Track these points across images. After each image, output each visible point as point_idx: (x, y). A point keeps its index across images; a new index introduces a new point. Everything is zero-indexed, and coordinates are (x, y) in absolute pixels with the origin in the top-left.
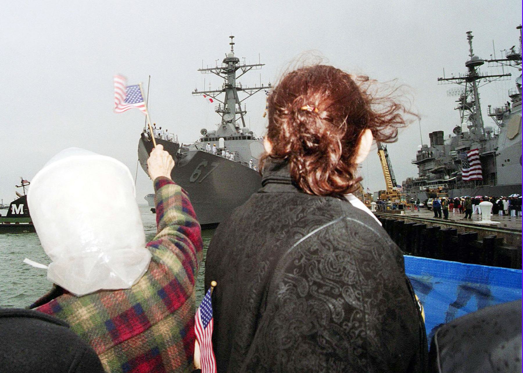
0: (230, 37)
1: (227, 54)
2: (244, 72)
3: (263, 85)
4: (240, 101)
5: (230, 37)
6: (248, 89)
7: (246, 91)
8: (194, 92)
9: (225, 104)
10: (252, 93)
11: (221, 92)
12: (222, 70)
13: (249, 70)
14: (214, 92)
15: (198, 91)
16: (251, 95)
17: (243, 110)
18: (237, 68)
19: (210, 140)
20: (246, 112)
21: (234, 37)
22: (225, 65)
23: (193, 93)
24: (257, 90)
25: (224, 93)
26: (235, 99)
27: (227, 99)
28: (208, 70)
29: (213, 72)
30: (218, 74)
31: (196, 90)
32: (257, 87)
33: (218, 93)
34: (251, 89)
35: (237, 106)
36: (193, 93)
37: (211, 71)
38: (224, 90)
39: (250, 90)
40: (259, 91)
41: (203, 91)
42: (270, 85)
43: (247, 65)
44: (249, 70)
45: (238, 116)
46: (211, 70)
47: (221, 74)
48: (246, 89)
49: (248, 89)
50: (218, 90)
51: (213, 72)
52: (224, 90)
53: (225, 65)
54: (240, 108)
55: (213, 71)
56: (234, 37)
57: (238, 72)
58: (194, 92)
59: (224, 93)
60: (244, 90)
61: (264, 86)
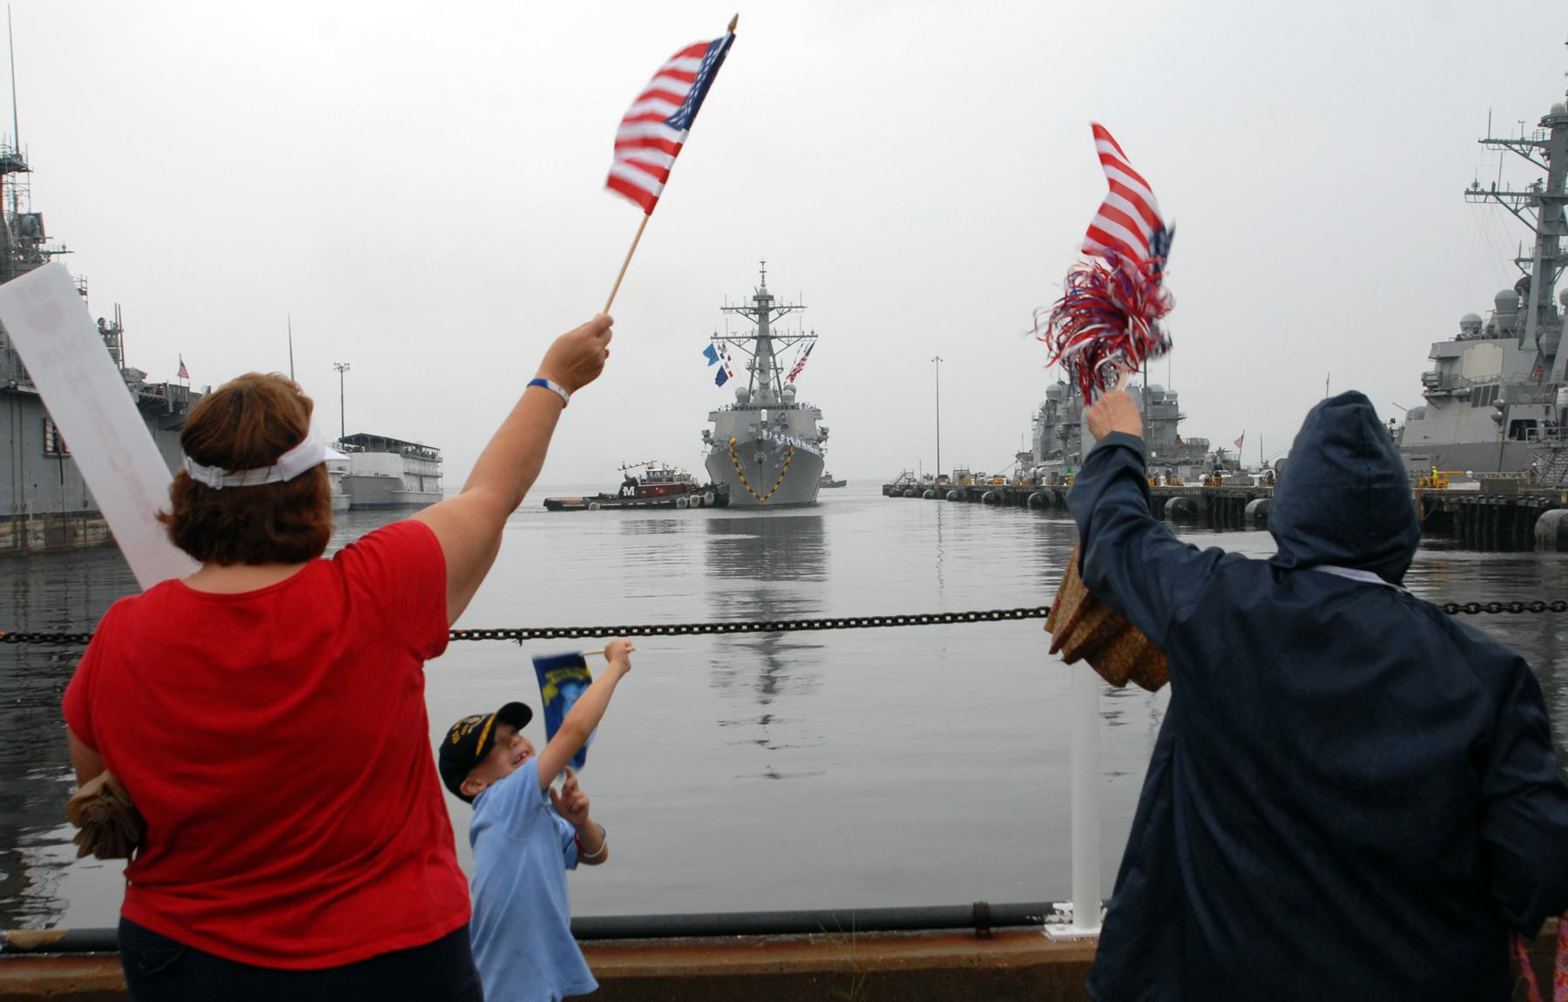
2: (781, 315)
4: (775, 352)
11: (750, 338)
15: (718, 336)
16: (789, 345)
17: (779, 366)
19: (747, 409)
22: (756, 305)
25: (756, 341)
30: (747, 315)
31: (716, 334)
33: (745, 340)
36: (712, 338)
41: (725, 336)
42: (812, 333)
43: (784, 305)
45: (772, 373)
46: (737, 309)
47: (750, 316)
53: (756, 305)
60: (779, 338)
61: (805, 334)
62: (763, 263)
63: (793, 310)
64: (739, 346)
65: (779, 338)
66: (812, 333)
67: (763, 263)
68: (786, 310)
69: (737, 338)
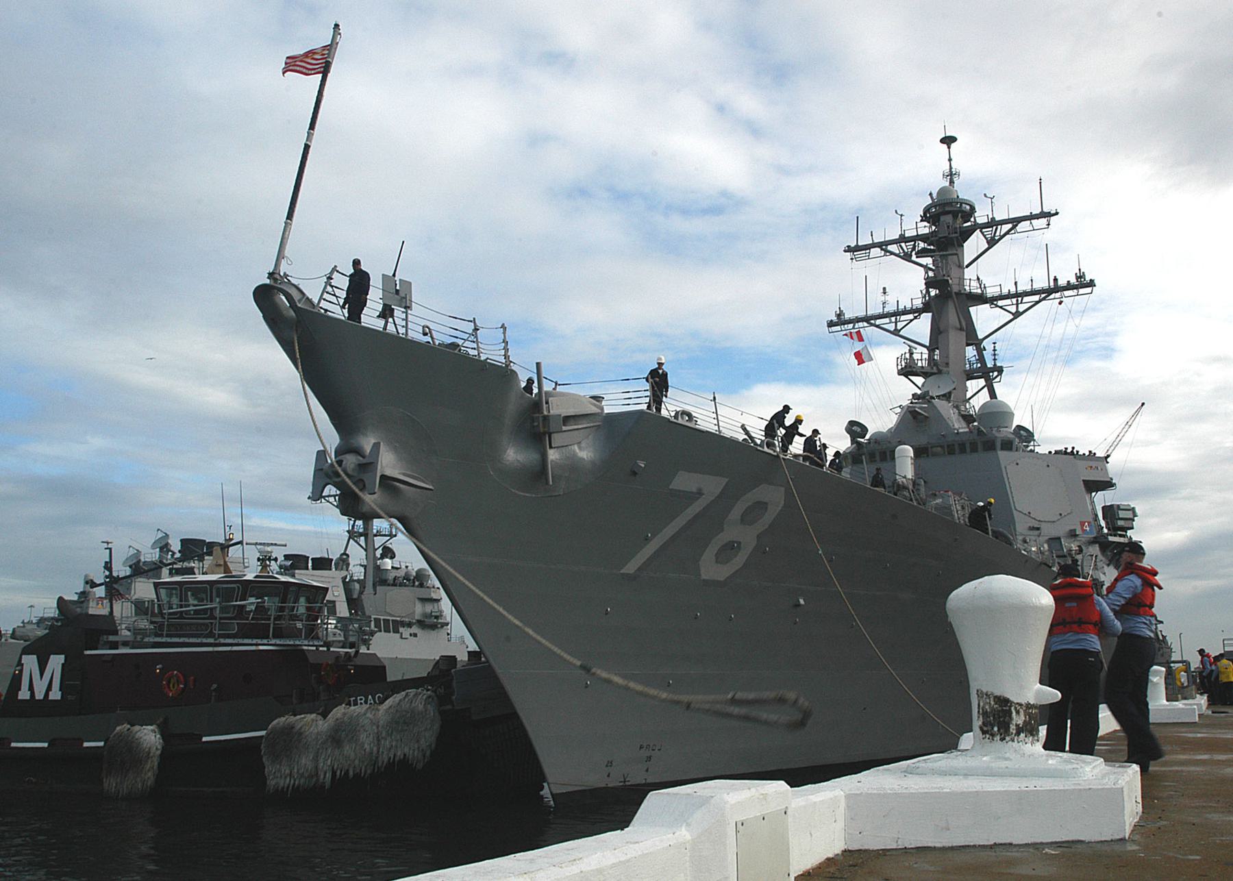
0: (943, 141)
1: (935, 196)
2: (992, 242)
3: (1056, 280)
5: (943, 141)
7: (1000, 303)
8: (835, 319)
9: (931, 349)
10: (1022, 308)
11: (917, 312)
12: (922, 245)
13: (1007, 233)
14: (896, 314)
15: (847, 316)
16: (1017, 315)
18: (967, 234)
20: (1000, 370)
22: (925, 228)
24: (1036, 298)
25: (926, 318)
26: (961, 329)
27: (937, 332)
28: (874, 245)
29: (892, 253)
30: (907, 257)
31: (839, 315)
32: (1037, 286)
34: (1017, 295)
35: (971, 352)
37: (886, 251)
38: (926, 308)
39: (1014, 300)
40: (1044, 299)
44: (1007, 233)
46: (882, 245)
49: (1008, 296)
51: (892, 253)
52: (926, 308)
53: (925, 228)
54: (981, 359)
55: (893, 248)
57: (973, 244)
58: (835, 319)
59: (926, 318)
60: (992, 301)
62: (948, 141)
63: (1024, 226)
64: (896, 332)
66: (1080, 277)
67: (948, 141)
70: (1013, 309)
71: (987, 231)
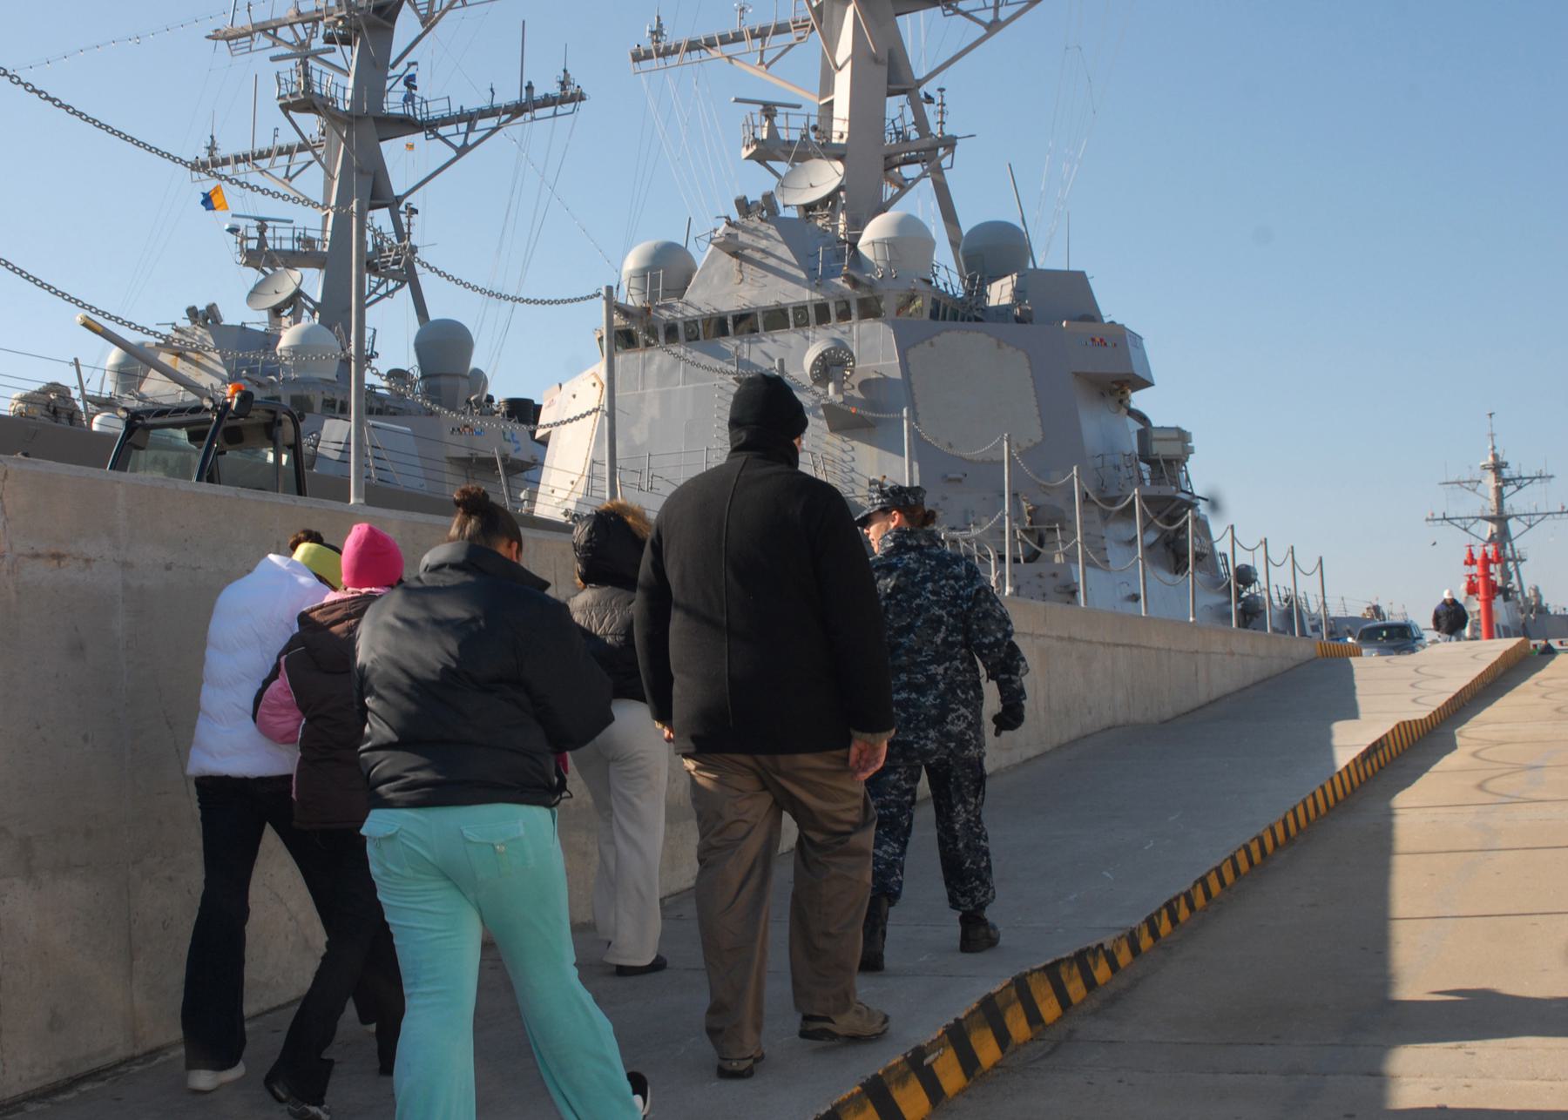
2: (1519, 488)
6: (1525, 515)
7: (1523, 518)
8: (1430, 517)
10: (1532, 523)
16: (1530, 526)
21: (1493, 413)
23: (1427, 520)
33: (1472, 521)
34: (1530, 514)
36: (1427, 520)
40: (1542, 519)
43: (1523, 476)
48: (1521, 515)
49: (1525, 515)
50: (1470, 515)
55: (1467, 485)
56: (1493, 413)
64: (1466, 530)
65: (1516, 516)
68: (1526, 481)
69: (1460, 518)
70: (1528, 523)
71: (1518, 482)
